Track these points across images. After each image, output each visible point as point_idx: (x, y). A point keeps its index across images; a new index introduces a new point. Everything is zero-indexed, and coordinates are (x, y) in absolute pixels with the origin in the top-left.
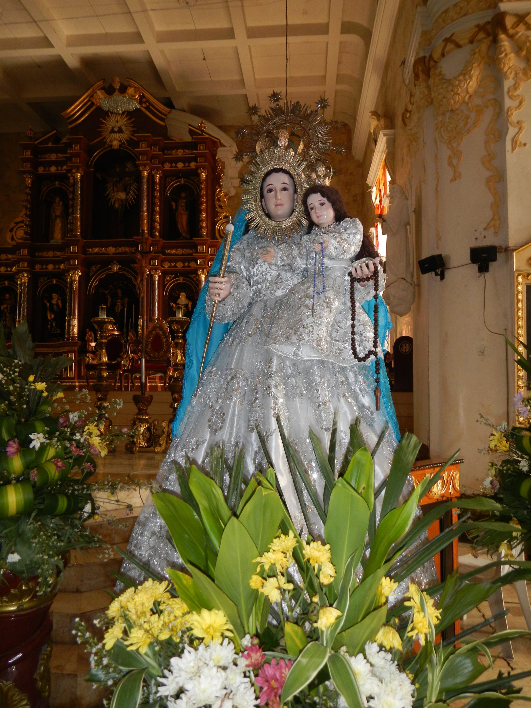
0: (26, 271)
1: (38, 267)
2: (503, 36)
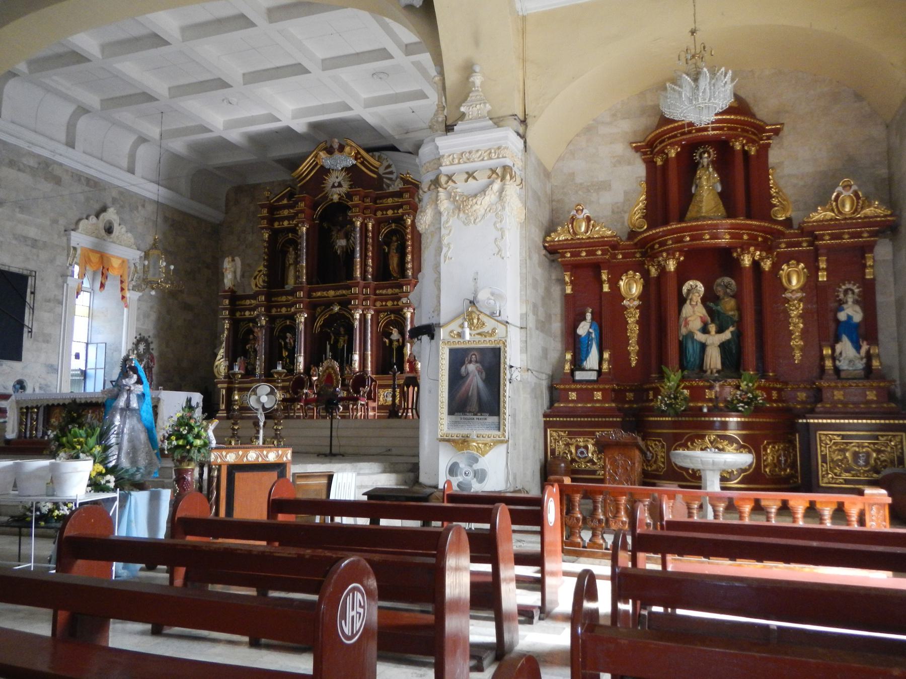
2: (440, 189)
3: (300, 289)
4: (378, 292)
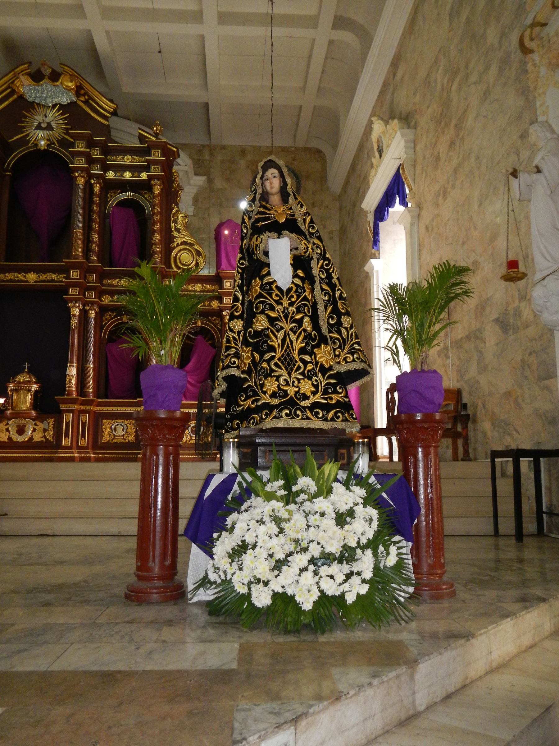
4: (105, 281)
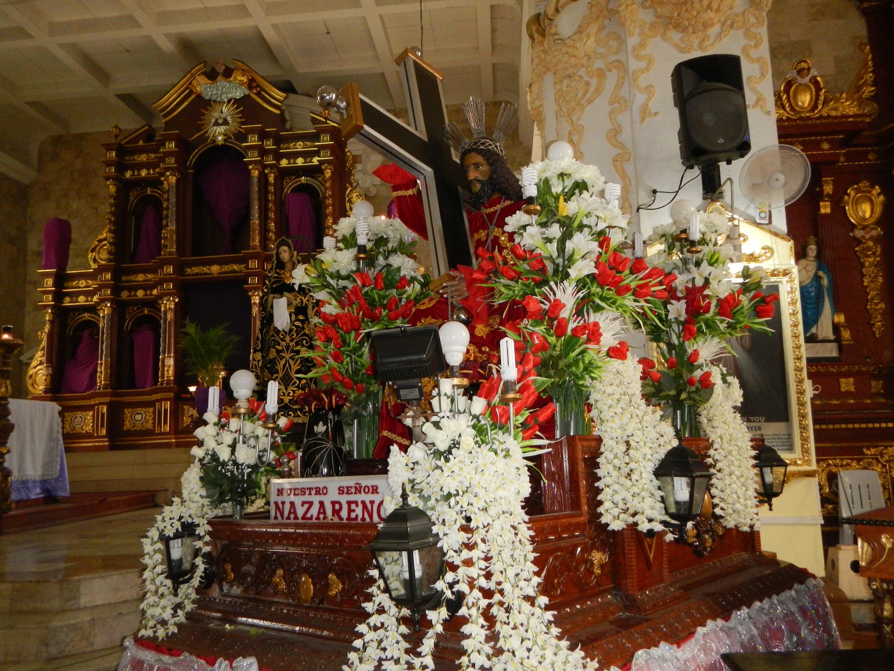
0: (108, 300)
1: (125, 295)
3: (168, 262)
